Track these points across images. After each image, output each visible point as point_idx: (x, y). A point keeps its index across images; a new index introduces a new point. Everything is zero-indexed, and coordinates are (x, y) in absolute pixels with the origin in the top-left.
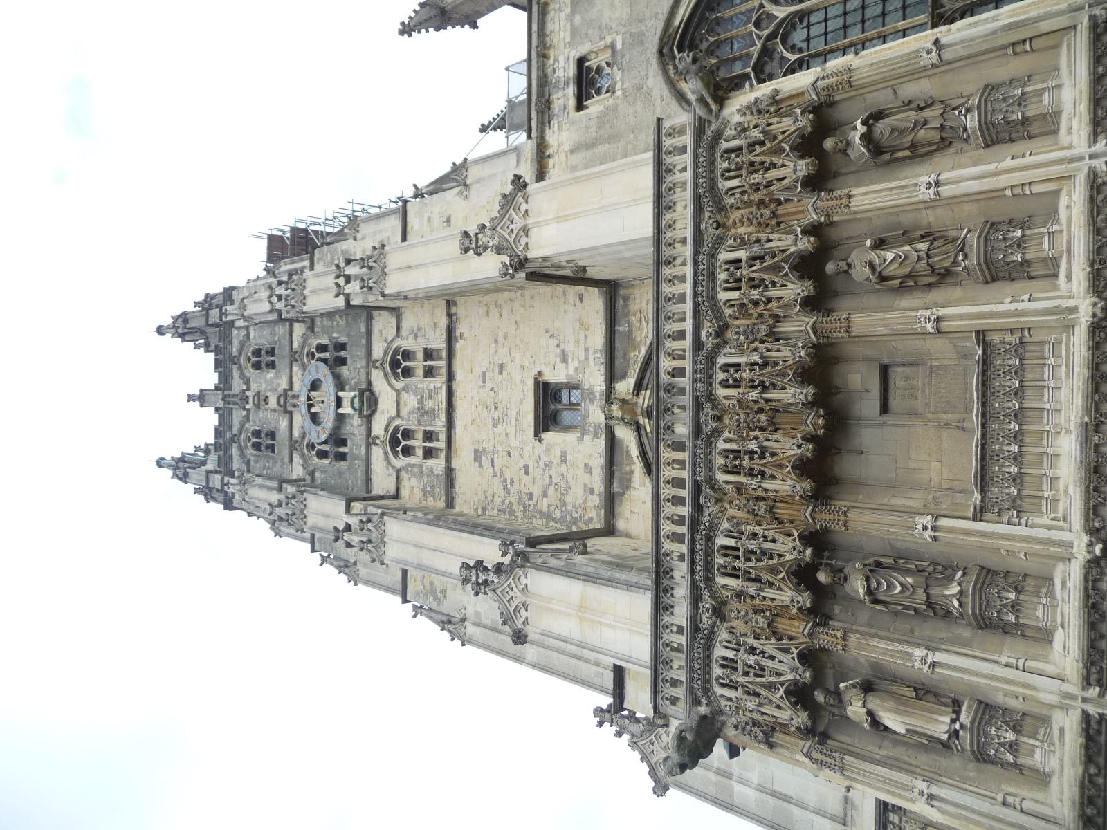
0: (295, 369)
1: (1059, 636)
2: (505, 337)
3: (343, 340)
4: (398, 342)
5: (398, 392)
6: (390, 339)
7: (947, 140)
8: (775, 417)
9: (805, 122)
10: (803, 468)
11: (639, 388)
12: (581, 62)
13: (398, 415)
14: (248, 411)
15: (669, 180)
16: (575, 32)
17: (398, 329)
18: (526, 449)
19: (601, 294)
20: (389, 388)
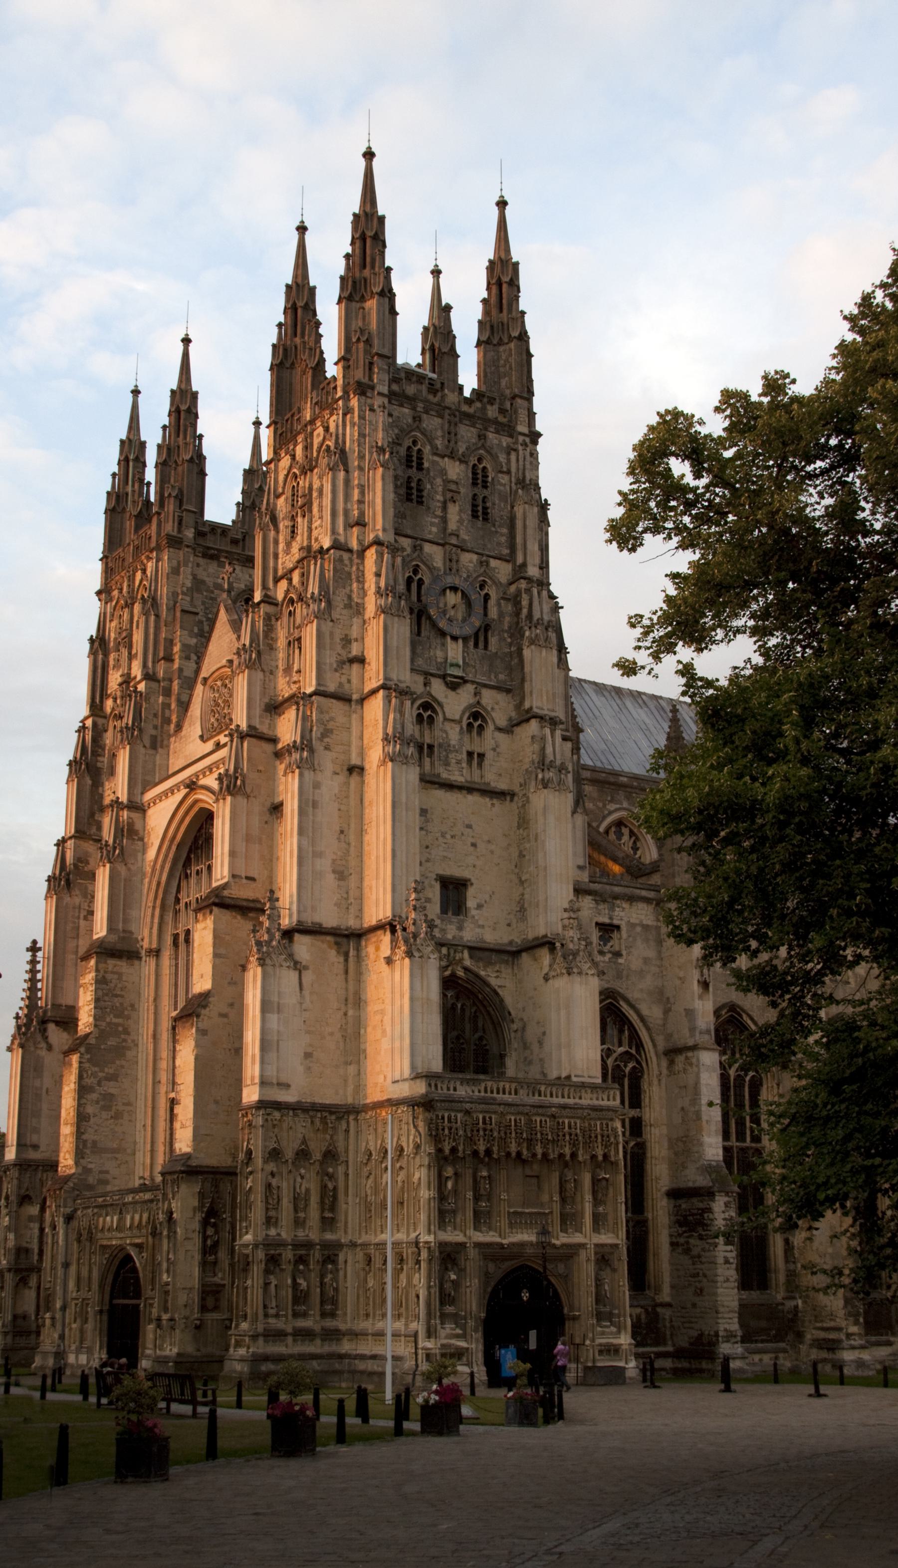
0: (475, 557)
1: (479, 1234)
2: (492, 852)
3: (493, 641)
4: (491, 727)
5: (459, 722)
6: (494, 714)
7: (596, 1202)
8: (530, 1142)
9: (613, 1159)
10: (519, 1154)
11: (466, 969)
12: (618, 927)
13: (445, 719)
14: (443, 457)
15: (600, 1092)
16: (633, 926)
17: (500, 730)
18: (429, 864)
19: (511, 943)
20: (462, 708)
